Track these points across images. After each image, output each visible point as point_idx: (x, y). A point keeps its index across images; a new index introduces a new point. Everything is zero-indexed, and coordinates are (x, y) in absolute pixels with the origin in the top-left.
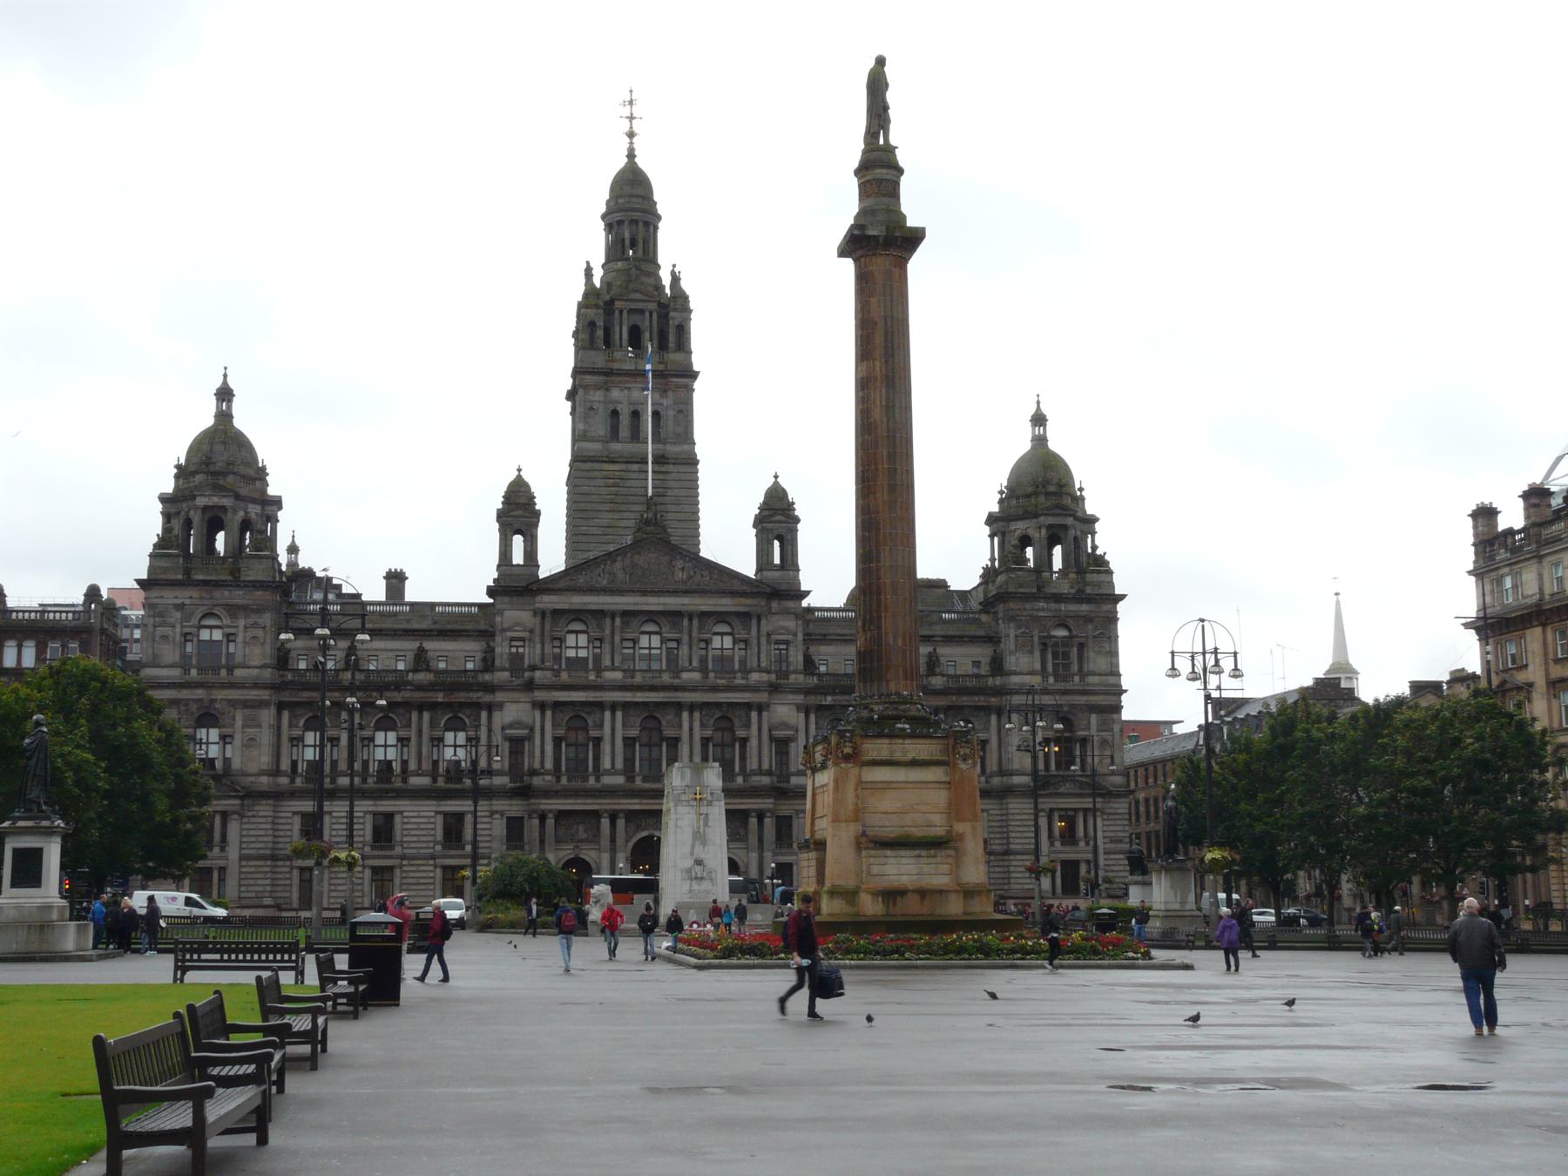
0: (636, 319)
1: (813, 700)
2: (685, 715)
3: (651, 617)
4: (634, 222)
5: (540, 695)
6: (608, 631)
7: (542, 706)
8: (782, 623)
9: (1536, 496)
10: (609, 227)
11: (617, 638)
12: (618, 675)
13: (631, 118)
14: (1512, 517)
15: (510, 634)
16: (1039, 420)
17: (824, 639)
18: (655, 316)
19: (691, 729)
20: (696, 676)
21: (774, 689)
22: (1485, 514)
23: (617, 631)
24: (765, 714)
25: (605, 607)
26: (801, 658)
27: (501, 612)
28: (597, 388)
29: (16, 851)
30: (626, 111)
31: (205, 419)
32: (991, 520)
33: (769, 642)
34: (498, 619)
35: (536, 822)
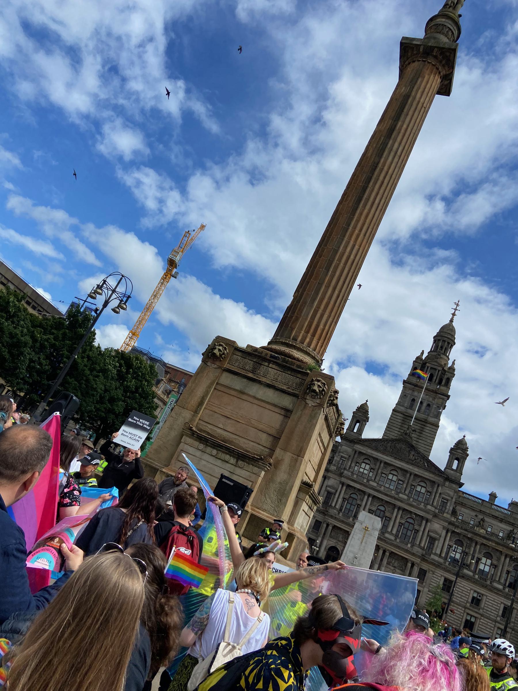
0: (433, 371)
1: (451, 528)
2: (396, 510)
3: (396, 468)
4: (444, 341)
5: (343, 480)
6: (377, 467)
7: (343, 484)
8: (447, 491)
10: (435, 341)
11: (380, 471)
12: (375, 484)
13: (456, 309)
15: (342, 454)
17: (463, 505)
18: (440, 372)
19: (396, 517)
20: (405, 497)
21: (435, 516)
23: (381, 468)
24: (429, 524)
25: (379, 458)
26: (451, 508)
27: (342, 445)
28: (410, 389)
30: (455, 307)
33: (439, 497)
34: (340, 448)
35: (325, 525)
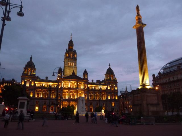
9: (160, 73)
14: (156, 75)
16: (110, 65)
22: (154, 75)
29: (20, 102)
31: (29, 60)
32: (105, 75)
